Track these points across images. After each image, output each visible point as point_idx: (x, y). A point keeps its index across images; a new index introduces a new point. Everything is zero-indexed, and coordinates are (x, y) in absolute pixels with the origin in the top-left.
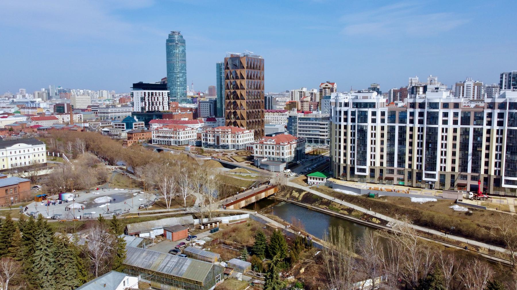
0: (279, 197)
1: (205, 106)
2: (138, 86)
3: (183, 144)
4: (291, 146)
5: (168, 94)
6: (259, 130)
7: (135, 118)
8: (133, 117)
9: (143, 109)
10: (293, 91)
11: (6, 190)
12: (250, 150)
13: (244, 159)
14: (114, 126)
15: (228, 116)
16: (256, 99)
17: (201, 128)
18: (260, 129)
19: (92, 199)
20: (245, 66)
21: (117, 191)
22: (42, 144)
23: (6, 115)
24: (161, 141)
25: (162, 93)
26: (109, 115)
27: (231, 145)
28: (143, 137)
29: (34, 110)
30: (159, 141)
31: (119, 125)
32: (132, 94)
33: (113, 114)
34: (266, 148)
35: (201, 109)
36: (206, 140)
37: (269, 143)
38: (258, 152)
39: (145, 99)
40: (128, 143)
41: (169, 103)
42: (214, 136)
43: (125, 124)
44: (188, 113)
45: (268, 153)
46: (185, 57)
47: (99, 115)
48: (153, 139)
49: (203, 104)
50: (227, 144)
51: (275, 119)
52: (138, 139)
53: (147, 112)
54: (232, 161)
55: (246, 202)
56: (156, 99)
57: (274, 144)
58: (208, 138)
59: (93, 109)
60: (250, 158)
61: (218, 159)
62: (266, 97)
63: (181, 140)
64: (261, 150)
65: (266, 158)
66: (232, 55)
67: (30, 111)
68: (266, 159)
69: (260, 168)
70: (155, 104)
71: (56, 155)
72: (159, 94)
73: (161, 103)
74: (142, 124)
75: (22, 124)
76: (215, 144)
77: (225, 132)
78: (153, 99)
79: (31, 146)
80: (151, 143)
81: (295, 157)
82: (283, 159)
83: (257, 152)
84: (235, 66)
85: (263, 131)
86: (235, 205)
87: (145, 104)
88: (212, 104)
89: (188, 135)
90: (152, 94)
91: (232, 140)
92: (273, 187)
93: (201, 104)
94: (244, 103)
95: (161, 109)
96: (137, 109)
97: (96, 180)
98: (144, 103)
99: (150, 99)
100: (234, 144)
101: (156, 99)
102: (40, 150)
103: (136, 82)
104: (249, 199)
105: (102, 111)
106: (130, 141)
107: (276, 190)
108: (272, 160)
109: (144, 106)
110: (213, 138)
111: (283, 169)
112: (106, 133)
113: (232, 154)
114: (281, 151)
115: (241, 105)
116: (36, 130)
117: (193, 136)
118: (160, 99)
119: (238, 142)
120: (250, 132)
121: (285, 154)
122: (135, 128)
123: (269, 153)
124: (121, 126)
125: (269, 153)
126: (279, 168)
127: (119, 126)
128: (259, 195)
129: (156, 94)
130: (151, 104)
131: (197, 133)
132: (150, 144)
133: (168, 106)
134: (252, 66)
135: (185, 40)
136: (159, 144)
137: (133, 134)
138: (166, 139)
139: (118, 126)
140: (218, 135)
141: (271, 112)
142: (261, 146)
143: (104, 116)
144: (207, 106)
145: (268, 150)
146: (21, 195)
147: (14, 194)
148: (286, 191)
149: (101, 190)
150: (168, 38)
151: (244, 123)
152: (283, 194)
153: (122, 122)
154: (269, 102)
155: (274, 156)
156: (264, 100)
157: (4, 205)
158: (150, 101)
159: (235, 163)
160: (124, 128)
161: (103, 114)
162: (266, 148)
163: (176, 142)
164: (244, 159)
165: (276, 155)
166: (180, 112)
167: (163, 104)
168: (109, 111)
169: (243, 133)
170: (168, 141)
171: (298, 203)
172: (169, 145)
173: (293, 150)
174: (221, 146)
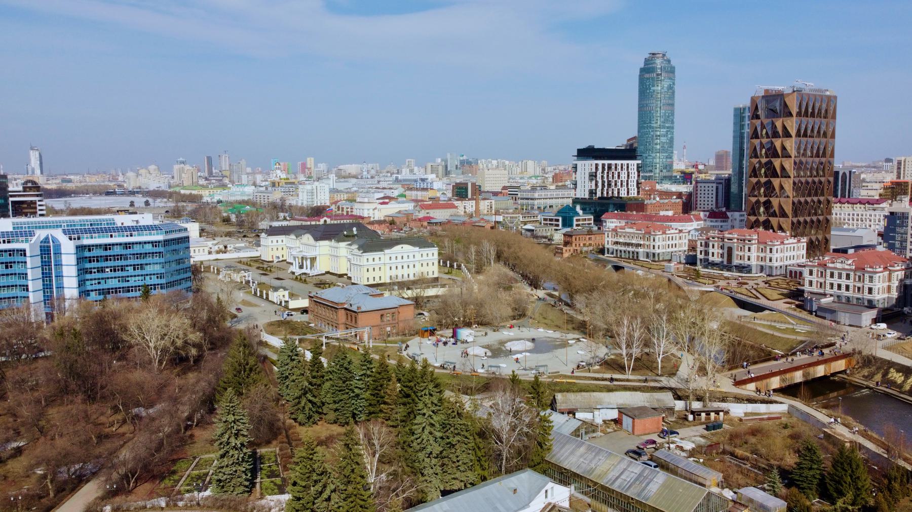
0: (857, 379)
1: (707, 189)
2: (587, 153)
3: (661, 259)
4: (890, 275)
5: (638, 167)
6: (817, 239)
7: (578, 208)
8: (575, 207)
9: (592, 193)
10: (903, 159)
11: (382, 315)
12: (796, 277)
13: (782, 294)
14: (543, 222)
15: (753, 208)
16: (815, 177)
17: (696, 230)
18: (820, 237)
19: (502, 343)
20: (794, 111)
21: (542, 333)
22: (434, 247)
23: (387, 201)
24: (621, 251)
25: (628, 164)
26: (536, 202)
27: (757, 265)
28: (590, 242)
29: (424, 193)
30: (617, 251)
31: (551, 220)
32: (575, 167)
33: (542, 201)
34: (832, 275)
35: (699, 195)
36: (707, 253)
37: (839, 266)
38: (814, 284)
39: (596, 176)
40: (564, 251)
41: (638, 183)
42: (722, 247)
43: (560, 219)
44: (673, 201)
45: (835, 287)
46: (674, 97)
47: (519, 201)
48: (606, 246)
49: (703, 185)
50: (747, 262)
51: (855, 217)
52: (582, 245)
53: (599, 198)
54: (757, 298)
55: (783, 380)
56: (616, 176)
57: (851, 270)
58: (711, 250)
59: (511, 191)
60: (796, 295)
61: (727, 291)
62: (837, 173)
63: (657, 251)
64: (822, 280)
65: (831, 295)
66: (766, 91)
67: (419, 193)
68: (832, 298)
69: (816, 315)
70: (613, 184)
71: (452, 266)
72: (622, 167)
73: (625, 184)
74: (589, 220)
75: (408, 215)
76: (722, 262)
77: (744, 240)
78: (610, 176)
79: (417, 249)
80: (604, 254)
81: (898, 299)
82: (870, 301)
83: (811, 283)
84: (773, 113)
85: (827, 241)
86: (759, 383)
87: (596, 185)
88: (720, 187)
89: (670, 242)
91: (758, 257)
92: (845, 356)
93: (699, 185)
94: (788, 185)
95: (623, 194)
96: (582, 192)
97: (509, 312)
98: (594, 182)
99: (605, 176)
100: (763, 263)
101: (616, 176)
102: (430, 256)
103: (583, 146)
104: (788, 376)
105: (525, 195)
106: (568, 248)
107: (849, 362)
108: (844, 300)
109: (594, 187)
110: (721, 251)
111: (869, 322)
112: (529, 234)
113: (758, 284)
114: (867, 284)
115: (782, 188)
116: (425, 224)
117: (680, 245)
118: (624, 176)
119: (771, 260)
120: (799, 241)
121: (875, 291)
122: (578, 225)
123: (839, 286)
124: (554, 223)
125: (839, 286)
126: (860, 318)
127: (550, 222)
128: (811, 370)
129: (616, 168)
130: (606, 184)
131: (689, 240)
132: (601, 256)
133: (636, 189)
134: (810, 110)
135: (674, 68)
136: (617, 257)
137: (574, 237)
138: (630, 249)
139: (548, 222)
140: (730, 245)
141: (848, 202)
142: (822, 272)
143: (527, 205)
144: (710, 189)
145: (836, 281)
146: (401, 325)
147: (391, 322)
148: (873, 369)
149: (516, 329)
150: (642, 65)
151: (786, 223)
152: (866, 374)
153: (556, 216)
154: (844, 182)
155: (850, 294)
156: (831, 179)
157: (377, 338)
158: (605, 179)
159: (763, 302)
160: (558, 225)
161: (525, 201)
162: (832, 275)
163: (648, 254)
164: (782, 294)
165: (854, 291)
166: (658, 199)
167: (627, 184)
168: (536, 195)
169: (782, 243)
170: (633, 252)
171: (902, 396)
172: (634, 260)
173: (895, 284)
174: (736, 266)
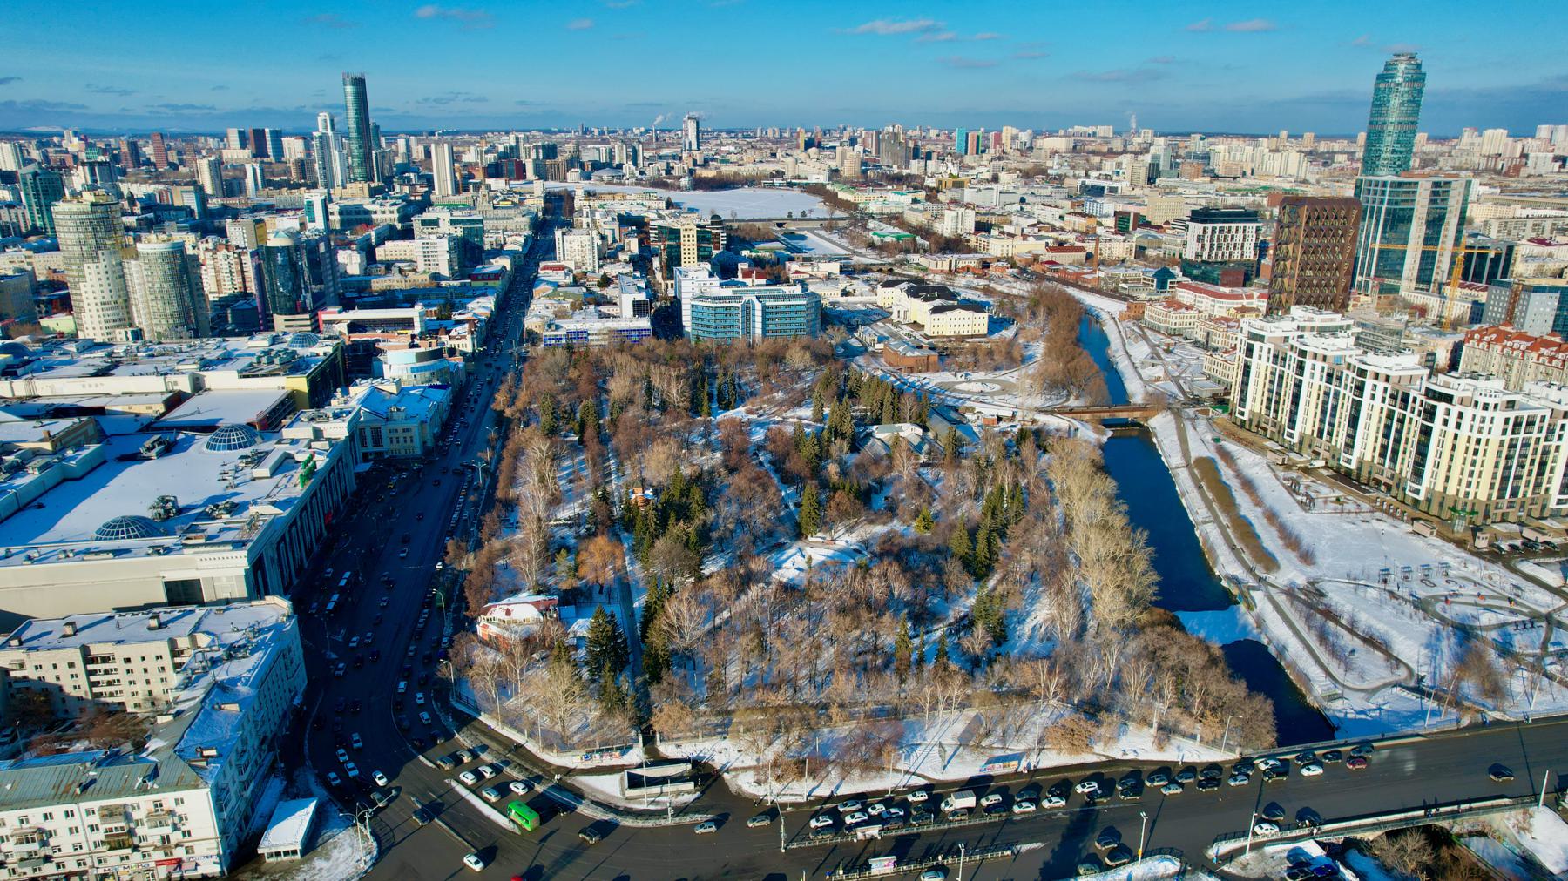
32: (1187, 228)
90: (1222, 230)
95: (1236, 256)
118: (1239, 239)
